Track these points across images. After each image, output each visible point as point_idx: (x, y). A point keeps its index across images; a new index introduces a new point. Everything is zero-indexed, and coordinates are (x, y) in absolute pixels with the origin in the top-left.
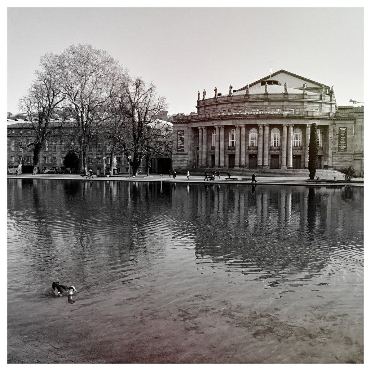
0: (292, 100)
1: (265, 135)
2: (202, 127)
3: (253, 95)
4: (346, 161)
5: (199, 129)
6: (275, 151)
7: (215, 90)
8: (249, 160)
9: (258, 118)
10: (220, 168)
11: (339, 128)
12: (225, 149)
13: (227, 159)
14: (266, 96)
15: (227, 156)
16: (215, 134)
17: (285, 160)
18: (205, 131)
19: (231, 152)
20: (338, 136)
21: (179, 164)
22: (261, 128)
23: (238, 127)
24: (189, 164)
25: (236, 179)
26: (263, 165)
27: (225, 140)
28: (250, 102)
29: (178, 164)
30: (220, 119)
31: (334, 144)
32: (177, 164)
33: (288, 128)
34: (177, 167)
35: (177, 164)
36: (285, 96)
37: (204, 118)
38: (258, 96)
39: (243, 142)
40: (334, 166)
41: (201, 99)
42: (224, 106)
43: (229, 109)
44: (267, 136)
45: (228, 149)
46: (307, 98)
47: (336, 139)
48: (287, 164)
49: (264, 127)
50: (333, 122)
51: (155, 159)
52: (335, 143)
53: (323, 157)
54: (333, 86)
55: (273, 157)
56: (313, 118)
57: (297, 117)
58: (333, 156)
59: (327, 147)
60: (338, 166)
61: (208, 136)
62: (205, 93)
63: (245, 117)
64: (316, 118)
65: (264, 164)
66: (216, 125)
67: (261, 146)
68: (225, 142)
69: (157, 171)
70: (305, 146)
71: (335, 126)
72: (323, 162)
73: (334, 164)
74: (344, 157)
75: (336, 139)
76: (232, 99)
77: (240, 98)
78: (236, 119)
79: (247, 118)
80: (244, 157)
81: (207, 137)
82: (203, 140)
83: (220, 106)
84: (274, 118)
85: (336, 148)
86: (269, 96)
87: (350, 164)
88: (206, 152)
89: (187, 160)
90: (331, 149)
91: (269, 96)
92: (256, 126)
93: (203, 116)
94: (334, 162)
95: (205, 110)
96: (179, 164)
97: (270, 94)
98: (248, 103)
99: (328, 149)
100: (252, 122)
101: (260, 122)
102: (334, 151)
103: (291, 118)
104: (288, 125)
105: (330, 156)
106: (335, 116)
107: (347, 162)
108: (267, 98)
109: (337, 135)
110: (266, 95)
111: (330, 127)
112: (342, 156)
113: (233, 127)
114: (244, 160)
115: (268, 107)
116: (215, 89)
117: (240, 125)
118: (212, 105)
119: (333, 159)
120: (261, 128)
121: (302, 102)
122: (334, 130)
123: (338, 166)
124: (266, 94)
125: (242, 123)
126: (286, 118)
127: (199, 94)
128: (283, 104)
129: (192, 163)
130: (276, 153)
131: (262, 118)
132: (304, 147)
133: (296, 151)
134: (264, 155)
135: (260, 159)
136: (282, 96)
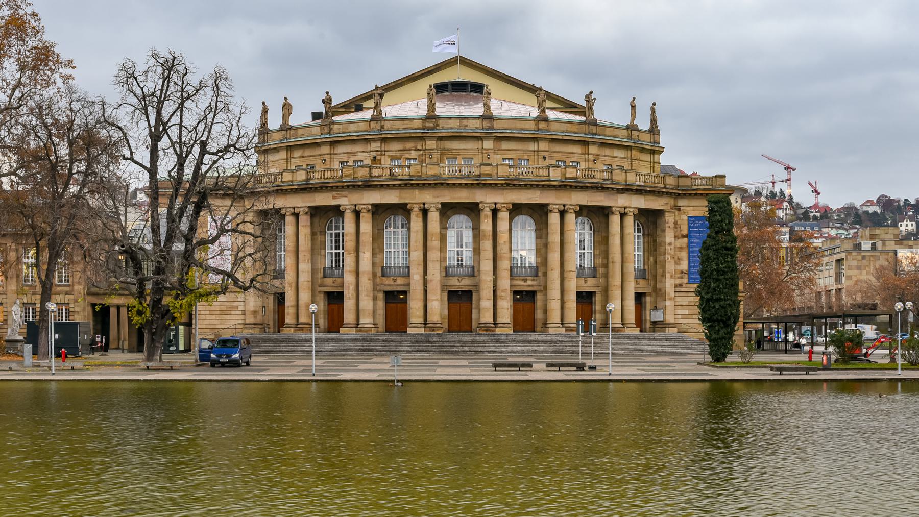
0: (560, 138)
1: (499, 233)
2: (296, 211)
3: (450, 118)
5: (284, 216)
6: (525, 280)
7: (323, 101)
8: (449, 309)
9: (478, 184)
10: (361, 331)
12: (374, 275)
13: (381, 304)
14: (486, 124)
15: (381, 296)
16: (343, 229)
17: (555, 305)
18: (304, 220)
19: (392, 283)
20: (686, 240)
21: (216, 322)
22: (487, 214)
23: (416, 209)
24: (248, 321)
25: (530, 366)
26: (496, 324)
27: (373, 249)
28: (440, 138)
29: (212, 322)
30: (359, 186)
31: (678, 261)
32: (206, 322)
33: (562, 214)
34: (208, 331)
35: (206, 322)
36: (542, 125)
37: (303, 181)
38: (465, 122)
39: (434, 255)
40: (680, 321)
41: (274, 122)
42: (358, 148)
43: (375, 158)
44: (503, 238)
45: (383, 276)
46: (596, 134)
47: (681, 248)
48: (562, 319)
49: (495, 212)
50: (671, 201)
51: (118, 308)
52: (679, 259)
53: (648, 299)
54: (654, 104)
55: (585, 298)
56: (627, 190)
57: (587, 184)
58: (677, 294)
59: (660, 271)
61: (313, 234)
62: (287, 107)
63: (440, 184)
64: (635, 188)
65: (499, 320)
66: (347, 203)
67: (486, 266)
68: (374, 254)
69: (126, 345)
70: (606, 266)
71: (677, 212)
72: (648, 313)
73: (680, 317)
75: (681, 248)
76: (382, 127)
77: (407, 124)
78: (412, 184)
79: (448, 184)
80: (437, 300)
81: (312, 239)
82: (301, 248)
83: (342, 149)
84: (526, 185)
85: (682, 272)
86: (496, 124)
88: (310, 283)
89: (241, 308)
90: (671, 277)
91: (496, 124)
92: (472, 210)
93: (301, 176)
94: (679, 312)
95: (288, 159)
96: (216, 322)
97: (499, 119)
98: (435, 142)
99: (663, 275)
100: (463, 196)
101: (486, 198)
102: (678, 281)
103: (571, 186)
104: (564, 205)
105: (669, 294)
106: (678, 186)
108: (492, 128)
109: (683, 236)
110: (488, 121)
111: (667, 214)
113: (403, 209)
114: (438, 308)
115: (494, 153)
116: (324, 96)
117: (424, 204)
118: (317, 145)
119: (677, 303)
120: (487, 214)
121: (585, 143)
122: (675, 223)
124: (488, 117)
125: (432, 199)
126: (560, 186)
127: (265, 111)
128: (536, 149)
129: (259, 319)
130: (529, 286)
131: (490, 184)
132: (601, 271)
133: (582, 282)
134: (499, 293)
135: (486, 303)
136: (532, 125)
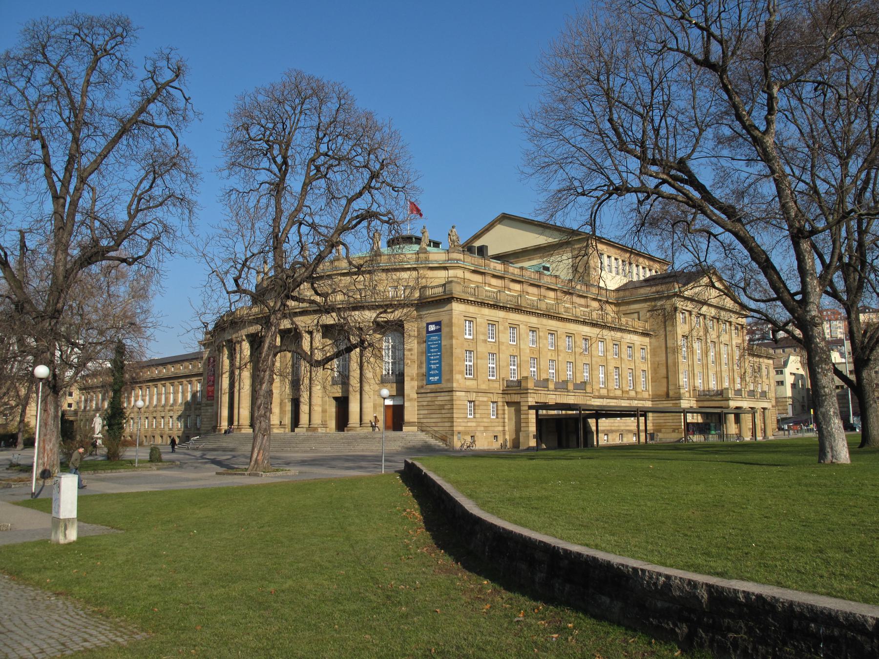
4: (442, 407)
11: (428, 324)
40: (422, 421)
58: (419, 395)
60: (429, 420)
73: (421, 416)
74: (439, 398)
75: (422, 353)
87: (449, 415)
90: (412, 379)
102: (420, 384)
105: (409, 396)
107: (443, 411)
112: (433, 395)
123: (429, 420)
